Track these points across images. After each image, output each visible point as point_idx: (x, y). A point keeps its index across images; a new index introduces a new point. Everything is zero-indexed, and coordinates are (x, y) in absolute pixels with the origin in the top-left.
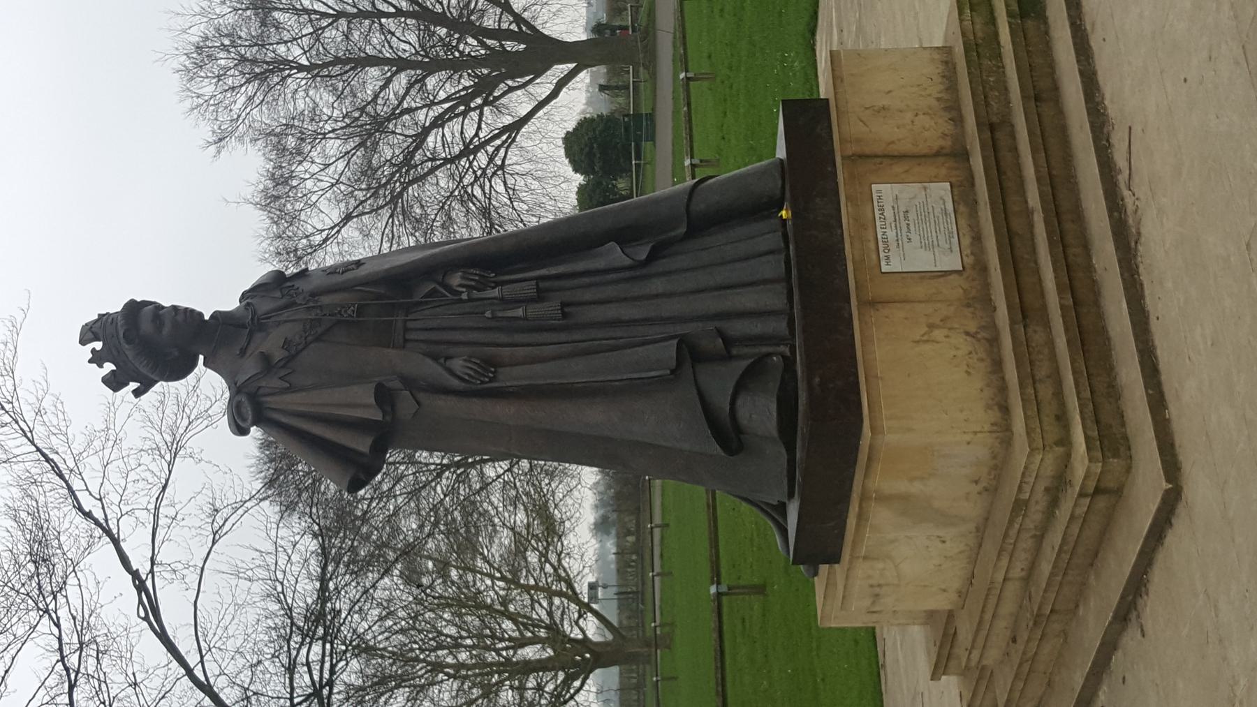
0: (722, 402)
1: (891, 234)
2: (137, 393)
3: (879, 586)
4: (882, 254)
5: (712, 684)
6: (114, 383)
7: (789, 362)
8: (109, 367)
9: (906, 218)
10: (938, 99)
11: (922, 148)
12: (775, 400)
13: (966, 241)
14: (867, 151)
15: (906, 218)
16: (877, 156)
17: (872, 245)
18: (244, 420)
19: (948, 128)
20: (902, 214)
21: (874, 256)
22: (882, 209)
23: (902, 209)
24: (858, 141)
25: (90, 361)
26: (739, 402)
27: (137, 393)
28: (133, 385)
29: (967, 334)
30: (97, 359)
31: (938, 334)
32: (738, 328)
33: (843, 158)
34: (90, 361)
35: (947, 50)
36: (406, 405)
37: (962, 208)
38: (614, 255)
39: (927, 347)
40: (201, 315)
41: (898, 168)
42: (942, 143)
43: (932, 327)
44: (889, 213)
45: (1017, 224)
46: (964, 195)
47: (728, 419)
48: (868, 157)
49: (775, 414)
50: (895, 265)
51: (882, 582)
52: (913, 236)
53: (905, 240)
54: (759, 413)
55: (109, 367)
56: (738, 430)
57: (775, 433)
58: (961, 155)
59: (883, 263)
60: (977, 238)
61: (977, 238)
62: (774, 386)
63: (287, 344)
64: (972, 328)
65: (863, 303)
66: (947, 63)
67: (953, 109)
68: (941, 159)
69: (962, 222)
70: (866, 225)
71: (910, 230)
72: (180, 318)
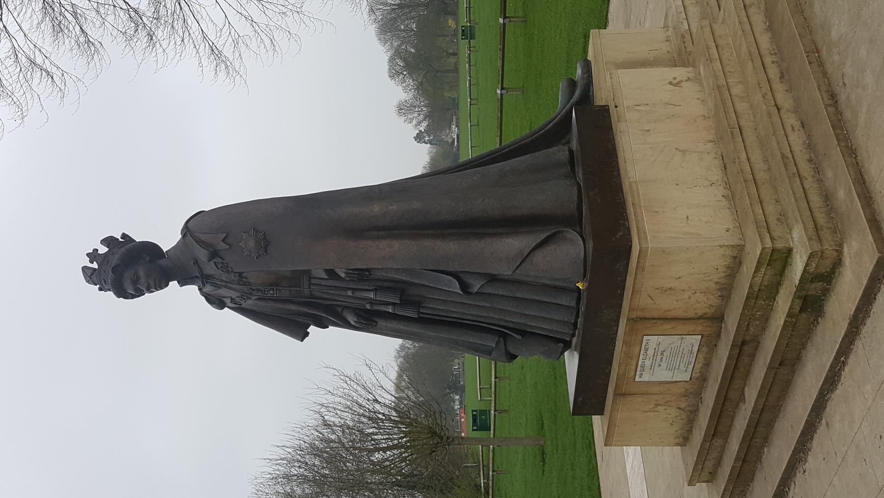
1: (648, 363)
4: (638, 373)
9: (662, 354)
10: (717, 283)
11: (691, 314)
13: (699, 366)
14: (648, 315)
15: (662, 354)
16: (654, 319)
17: (633, 368)
19: (715, 301)
20: (659, 353)
21: (632, 373)
22: (646, 350)
23: (661, 349)
24: (643, 309)
25: (88, 255)
29: (679, 408)
31: (660, 408)
33: (628, 320)
34: (88, 255)
37: (705, 349)
39: (651, 414)
41: (667, 326)
42: (707, 311)
43: (657, 405)
44: (650, 352)
45: (732, 395)
46: (710, 343)
48: (646, 319)
50: (646, 378)
52: (664, 365)
53: (657, 365)
58: (717, 318)
59: (637, 377)
60: (707, 364)
61: (707, 364)
64: (683, 405)
65: (617, 394)
66: (735, 257)
67: (726, 290)
68: (701, 321)
69: (701, 356)
70: (631, 357)
71: (662, 360)
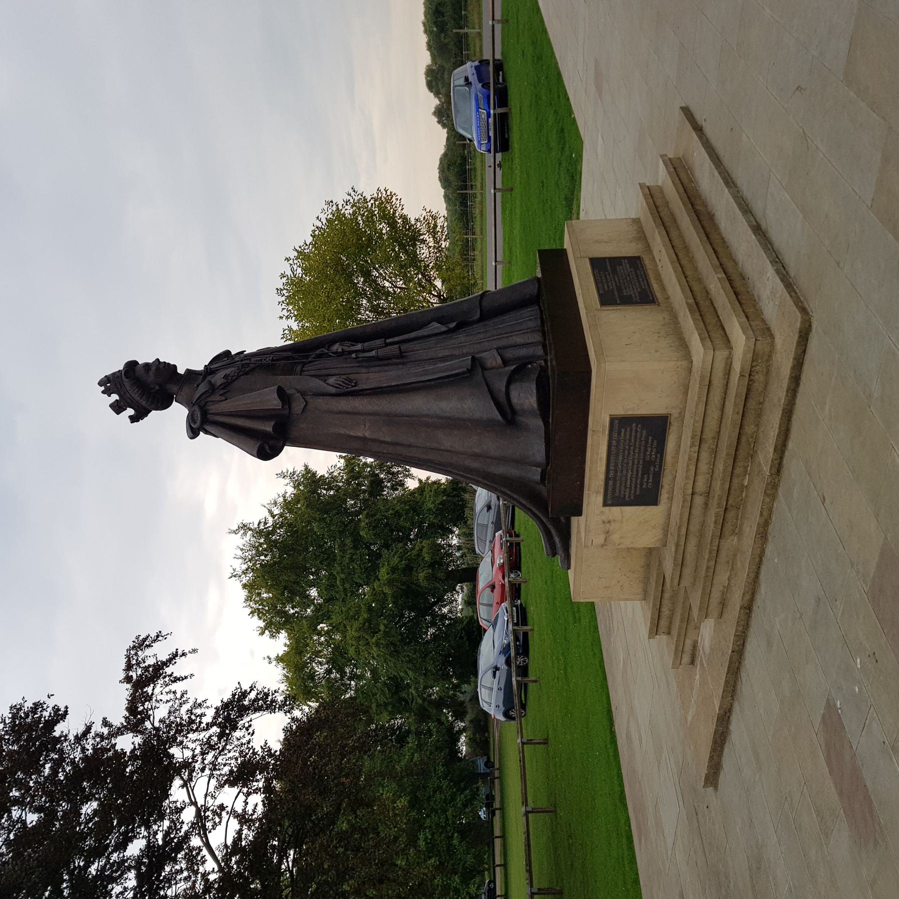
0: (500, 385)
2: (134, 419)
3: (609, 522)
5: (520, 795)
6: (117, 408)
7: (543, 370)
8: (115, 397)
12: (534, 387)
18: (195, 423)
26: (512, 387)
27: (134, 419)
28: (130, 412)
30: (108, 392)
32: (509, 354)
35: (637, 221)
36: (298, 406)
38: (436, 327)
40: (175, 367)
47: (506, 403)
49: (535, 392)
51: (610, 518)
54: (525, 397)
55: (115, 397)
56: (514, 411)
57: (535, 406)
62: (534, 377)
63: (226, 377)
72: (161, 366)
